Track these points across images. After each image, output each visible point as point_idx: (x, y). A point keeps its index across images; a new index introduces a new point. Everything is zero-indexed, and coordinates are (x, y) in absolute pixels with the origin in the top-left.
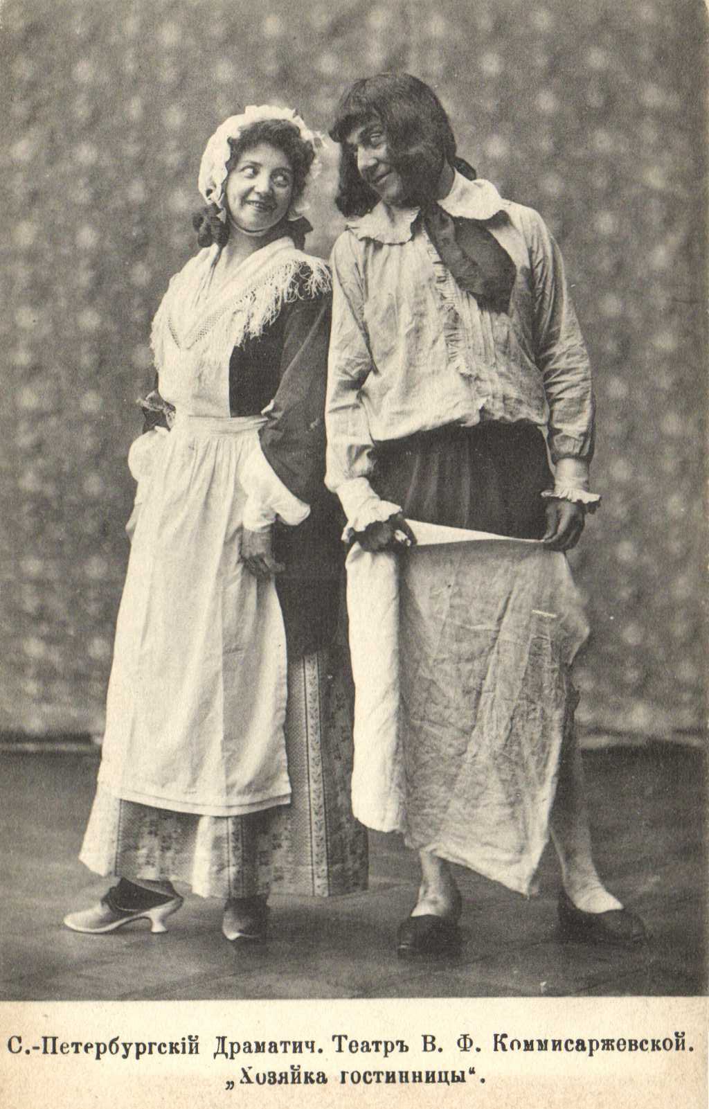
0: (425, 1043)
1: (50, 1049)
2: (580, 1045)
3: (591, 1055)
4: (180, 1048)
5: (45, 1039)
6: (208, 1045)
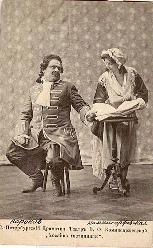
1: (7, 228)
4: (35, 228)
5: (7, 226)
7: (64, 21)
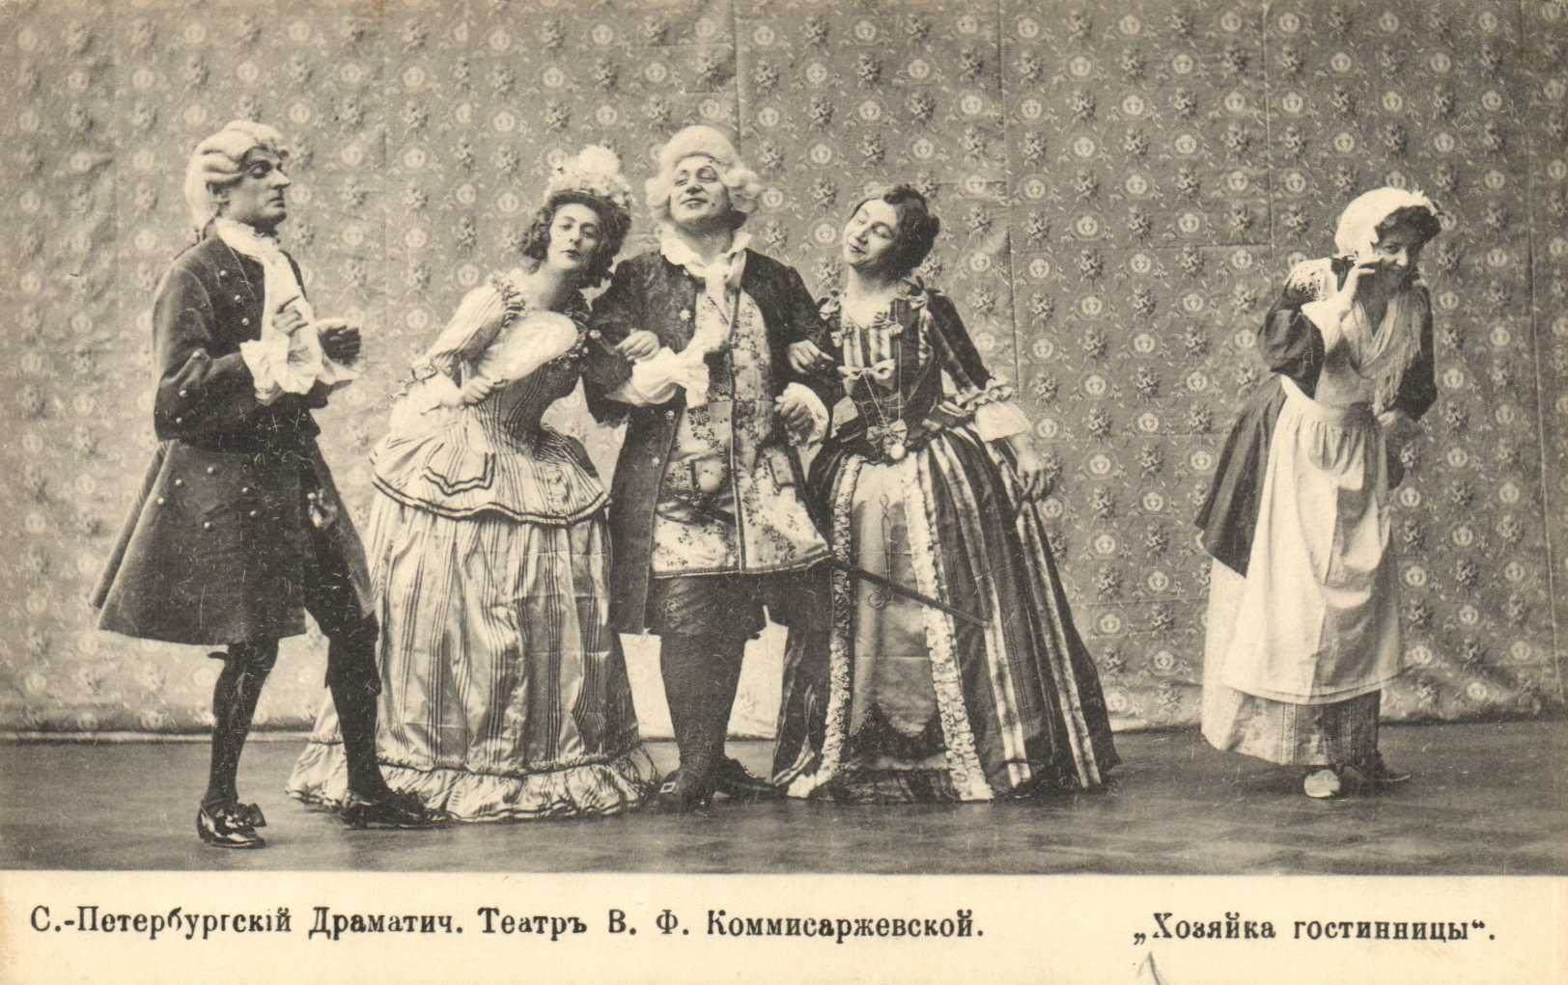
0: (612, 920)
1: (88, 924)
2: (826, 928)
3: (840, 941)
4: (263, 923)
5: (82, 909)
6: (303, 919)
7: (720, 76)
